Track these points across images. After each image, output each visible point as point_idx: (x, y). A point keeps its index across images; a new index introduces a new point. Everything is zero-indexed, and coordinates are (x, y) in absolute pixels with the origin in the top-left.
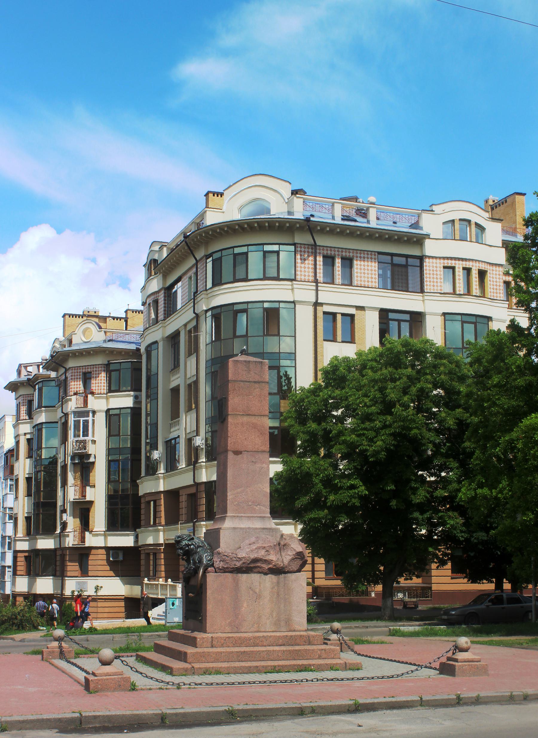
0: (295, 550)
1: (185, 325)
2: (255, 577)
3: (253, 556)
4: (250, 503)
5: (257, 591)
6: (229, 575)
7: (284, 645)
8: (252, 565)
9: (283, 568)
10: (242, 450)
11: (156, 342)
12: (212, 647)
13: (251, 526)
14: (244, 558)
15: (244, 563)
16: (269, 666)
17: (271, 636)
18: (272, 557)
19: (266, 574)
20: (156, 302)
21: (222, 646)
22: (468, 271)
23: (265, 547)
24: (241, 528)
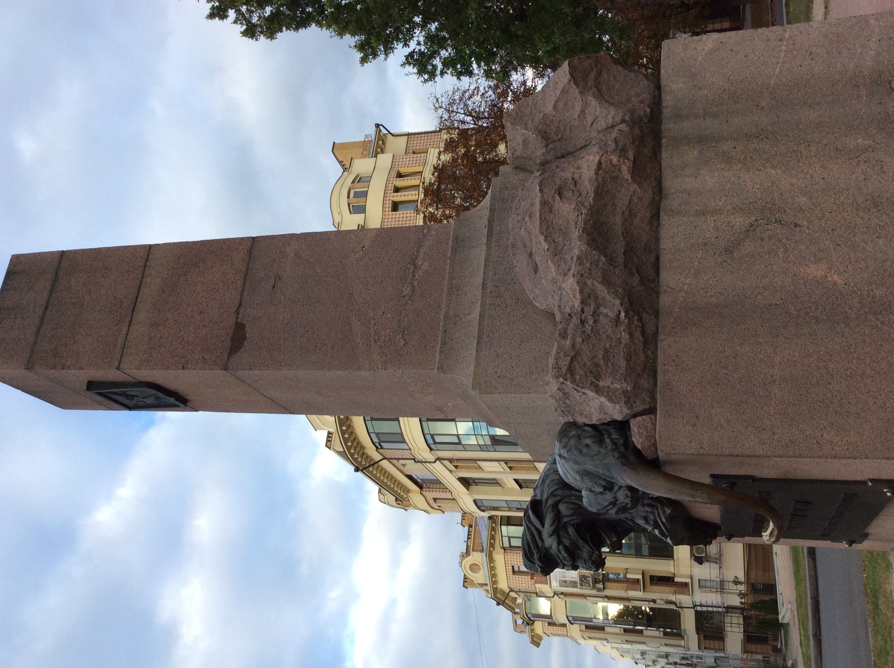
0: (564, 91)
1: (451, 471)
2: (674, 233)
3: (576, 246)
4: (407, 291)
5: (740, 221)
6: (667, 347)
8: (620, 247)
9: (634, 122)
10: (232, 322)
11: (475, 501)
13: (480, 280)
14: (582, 285)
15: (607, 282)
18: (586, 166)
20: (435, 500)
22: (397, 190)
23: (544, 203)
24: (481, 316)
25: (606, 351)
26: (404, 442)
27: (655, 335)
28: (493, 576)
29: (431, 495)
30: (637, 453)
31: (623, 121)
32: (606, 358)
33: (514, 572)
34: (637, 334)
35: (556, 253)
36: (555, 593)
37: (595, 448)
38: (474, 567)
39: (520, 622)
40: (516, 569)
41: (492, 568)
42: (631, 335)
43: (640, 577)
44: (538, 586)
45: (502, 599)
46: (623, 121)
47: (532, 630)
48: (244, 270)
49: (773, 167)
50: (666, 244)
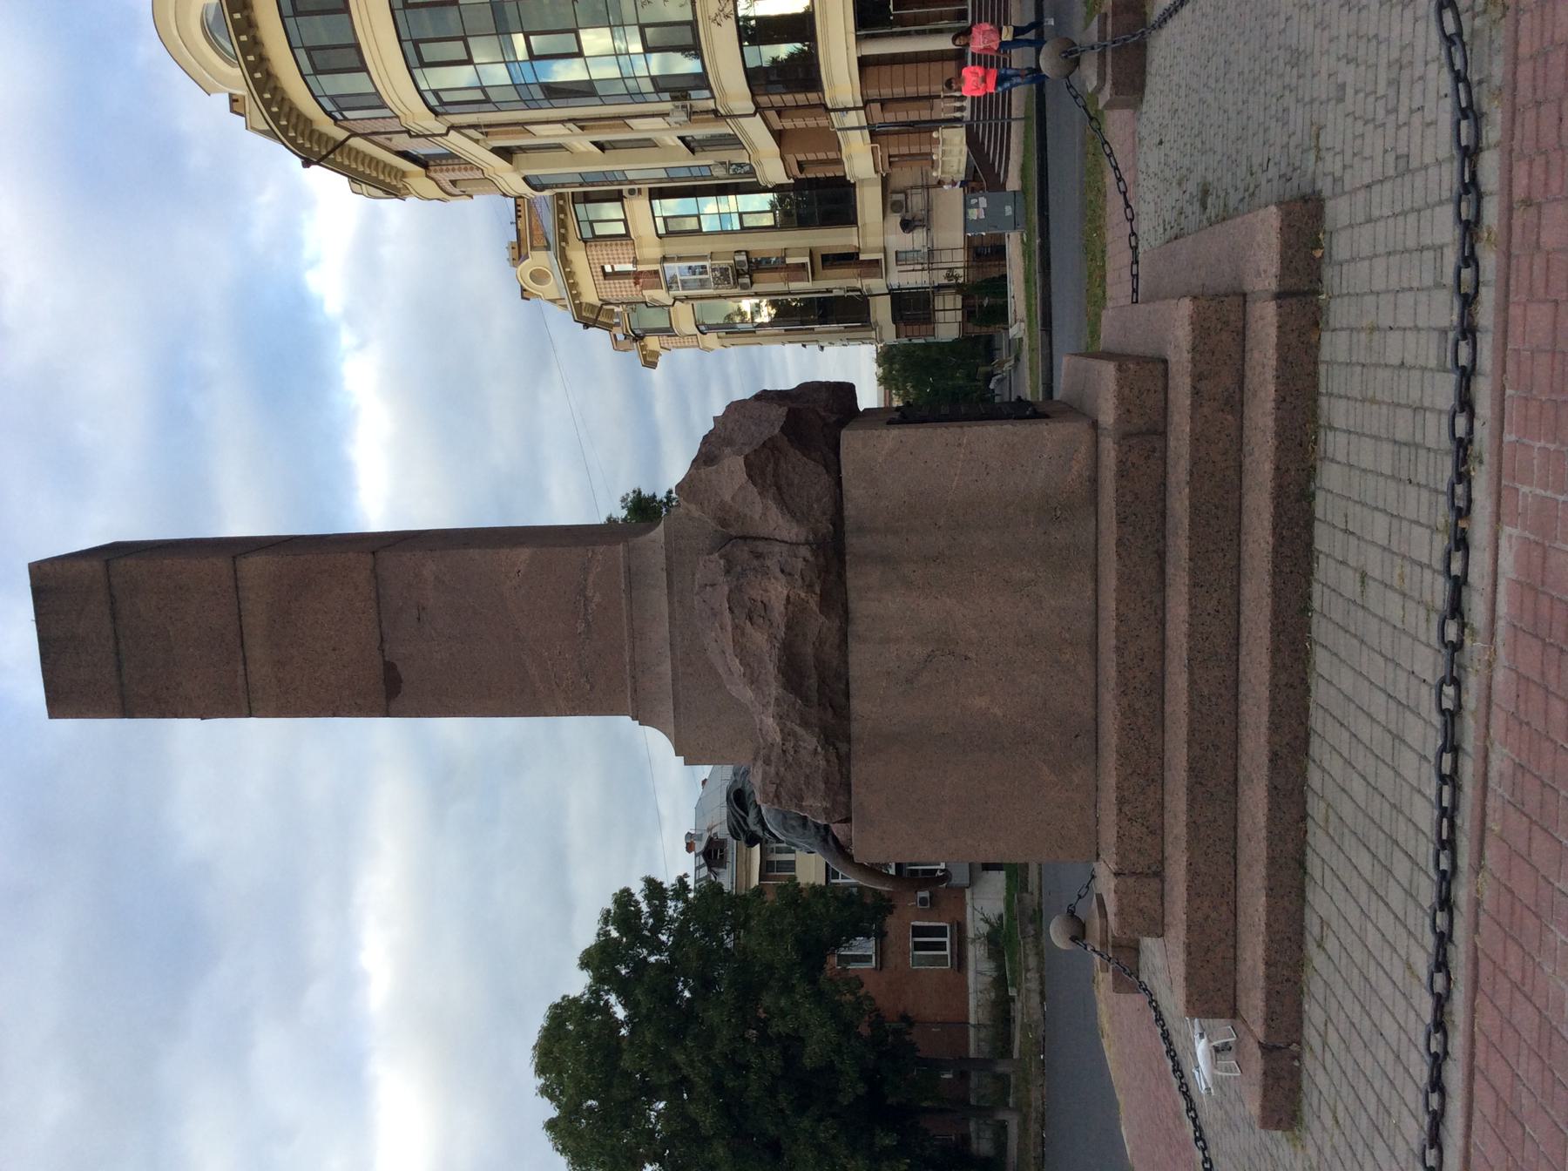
0: (741, 488)
1: (477, 141)
2: (862, 660)
3: (774, 689)
4: (581, 627)
5: (920, 652)
6: (859, 771)
7: (1161, 555)
8: (813, 682)
11: (525, 179)
12: (1159, 875)
15: (805, 723)
16: (1273, 699)
17: (1121, 618)
18: (777, 592)
19: (846, 616)
20: (454, 183)
21: (1158, 832)
23: (736, 627)
25: (807, 777)
26: (383, 106)
27: (848, 755)
28: (572, 285)
29: (444, 177)
30: (835, 839)
31: (807, 543)
32: (807, 784)
33: (605, 275)
34: (833, 759)
35: (753, 680)
36: (675, 299)
37: (800, 830)
38: (538, 276)
39: (620, 337)
40: (608, 269)
41: (569, 275)
42: (828, 761)
43: (806, 260)
44: (645, 292)
45: (590, 317)
46: (807, 543)
47: (643, 348)
48: (373, 595)
49: (949, 596)
50: (854, 672)
